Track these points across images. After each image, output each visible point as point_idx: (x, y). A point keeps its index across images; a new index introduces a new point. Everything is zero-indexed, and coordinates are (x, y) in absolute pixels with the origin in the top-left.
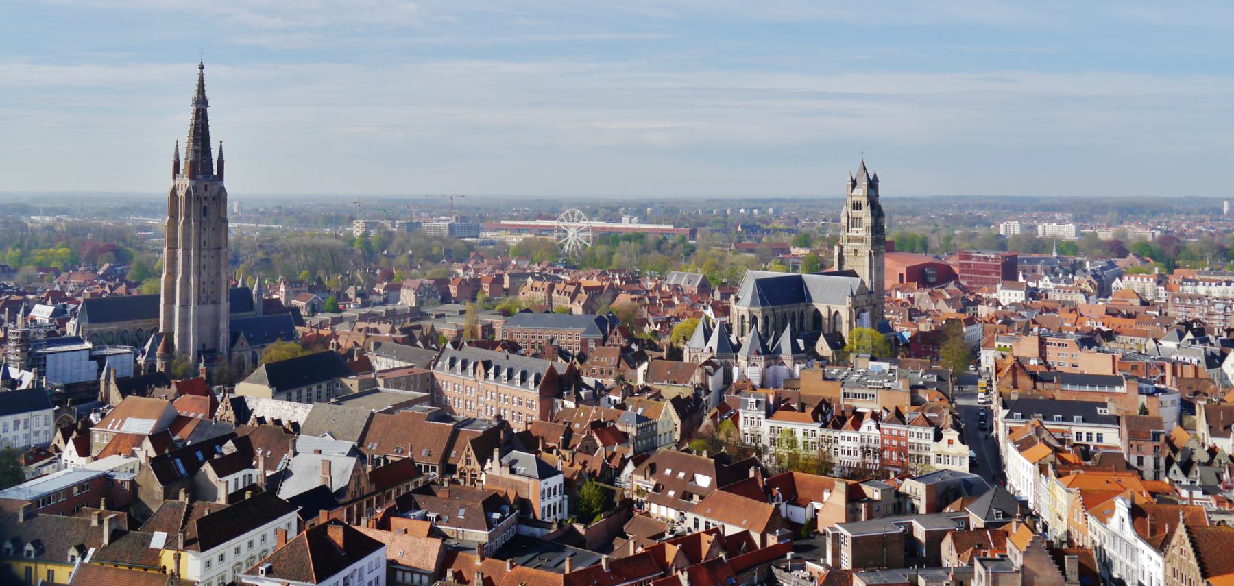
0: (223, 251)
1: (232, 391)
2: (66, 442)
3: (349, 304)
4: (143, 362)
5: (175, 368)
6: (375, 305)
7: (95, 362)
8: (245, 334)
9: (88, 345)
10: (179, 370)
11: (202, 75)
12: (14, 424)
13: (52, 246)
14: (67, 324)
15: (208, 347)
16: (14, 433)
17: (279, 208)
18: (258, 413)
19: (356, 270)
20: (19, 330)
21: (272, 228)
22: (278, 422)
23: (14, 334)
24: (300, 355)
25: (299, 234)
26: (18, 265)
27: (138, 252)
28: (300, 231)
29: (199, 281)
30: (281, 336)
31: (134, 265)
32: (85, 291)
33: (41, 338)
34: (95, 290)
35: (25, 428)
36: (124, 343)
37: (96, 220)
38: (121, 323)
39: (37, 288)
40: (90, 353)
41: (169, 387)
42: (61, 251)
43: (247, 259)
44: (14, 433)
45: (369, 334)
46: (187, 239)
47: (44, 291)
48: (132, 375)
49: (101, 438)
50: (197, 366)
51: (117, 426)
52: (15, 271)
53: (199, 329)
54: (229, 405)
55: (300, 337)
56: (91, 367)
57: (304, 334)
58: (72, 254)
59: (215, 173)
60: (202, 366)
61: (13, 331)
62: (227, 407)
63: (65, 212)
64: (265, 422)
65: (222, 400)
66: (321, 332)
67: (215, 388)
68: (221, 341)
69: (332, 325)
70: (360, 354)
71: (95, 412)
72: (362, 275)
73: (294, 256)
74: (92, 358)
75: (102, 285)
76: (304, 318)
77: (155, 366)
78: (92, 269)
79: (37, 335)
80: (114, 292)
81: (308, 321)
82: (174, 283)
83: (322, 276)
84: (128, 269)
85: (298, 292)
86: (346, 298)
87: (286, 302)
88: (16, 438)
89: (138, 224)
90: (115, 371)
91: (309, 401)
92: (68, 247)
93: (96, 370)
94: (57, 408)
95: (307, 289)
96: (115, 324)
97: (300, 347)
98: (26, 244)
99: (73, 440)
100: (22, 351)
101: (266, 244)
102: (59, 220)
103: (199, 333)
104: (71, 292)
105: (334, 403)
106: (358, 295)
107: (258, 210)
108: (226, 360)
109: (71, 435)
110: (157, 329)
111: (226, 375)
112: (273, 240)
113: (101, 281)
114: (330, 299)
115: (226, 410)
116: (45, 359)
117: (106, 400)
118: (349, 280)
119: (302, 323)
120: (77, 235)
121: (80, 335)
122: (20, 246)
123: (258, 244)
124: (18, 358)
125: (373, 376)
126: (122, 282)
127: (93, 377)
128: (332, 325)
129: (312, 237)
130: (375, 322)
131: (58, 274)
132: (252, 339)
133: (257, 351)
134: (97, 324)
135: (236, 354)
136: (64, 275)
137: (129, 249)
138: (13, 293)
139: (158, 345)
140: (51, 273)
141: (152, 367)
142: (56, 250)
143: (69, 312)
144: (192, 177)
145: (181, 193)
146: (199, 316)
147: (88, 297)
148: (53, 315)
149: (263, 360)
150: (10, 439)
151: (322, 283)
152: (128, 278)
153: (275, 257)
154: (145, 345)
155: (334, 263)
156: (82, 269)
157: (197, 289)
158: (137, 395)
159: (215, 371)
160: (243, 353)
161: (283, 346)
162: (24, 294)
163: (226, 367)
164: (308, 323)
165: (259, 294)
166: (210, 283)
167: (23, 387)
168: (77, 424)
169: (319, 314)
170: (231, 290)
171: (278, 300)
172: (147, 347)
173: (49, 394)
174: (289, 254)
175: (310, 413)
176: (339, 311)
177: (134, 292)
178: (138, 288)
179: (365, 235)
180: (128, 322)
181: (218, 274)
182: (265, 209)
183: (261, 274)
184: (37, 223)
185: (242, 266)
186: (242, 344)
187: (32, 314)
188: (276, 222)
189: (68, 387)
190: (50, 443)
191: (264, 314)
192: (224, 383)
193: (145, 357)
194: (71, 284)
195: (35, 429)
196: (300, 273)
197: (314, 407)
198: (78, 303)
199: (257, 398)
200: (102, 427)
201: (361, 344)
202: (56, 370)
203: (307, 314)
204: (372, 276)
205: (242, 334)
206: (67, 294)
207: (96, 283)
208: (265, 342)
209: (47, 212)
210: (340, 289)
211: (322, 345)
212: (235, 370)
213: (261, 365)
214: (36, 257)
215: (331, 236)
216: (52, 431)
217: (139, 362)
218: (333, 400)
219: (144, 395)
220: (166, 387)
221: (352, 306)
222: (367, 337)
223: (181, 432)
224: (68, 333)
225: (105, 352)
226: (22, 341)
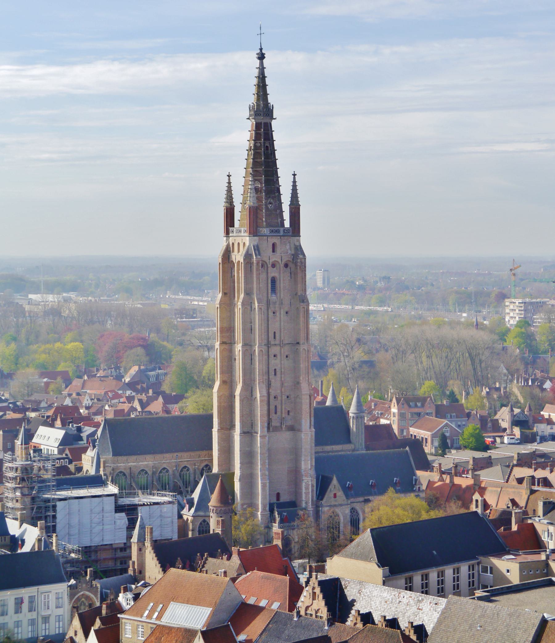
0: (303, 347)
1: (322, 569)
2: (86, 635)
3: (501, 437)
4: (190, 518)
5: (237, 528)
6: (543, 439)
7: (123, 514)
8: (339, 481)
9: (113, 489)
10: (242, 533)
11: (262, 69)
12: (16, 604)
13: (59, 340)
14: (83, 456)
15: (284, 498)
16: (16, 617)
17: (387, 279)
18: (361, 606)
19: (511, 381)
20: (20, 462)
21: (375, 313)
22: (393, 623)
23: (11, 469)
24: (425, 516)
25: (418, 322)
26: (13, 367)
27: (180, 348)
28: (420, 317)
29: (269, 394)
30: (394, 485)
31: (173, 369)
32: (107, 407)
33: (48, 476)
34: (120, 407)
35: (30, 610)
36: (163, 487)
37: (117, 300)
38: (158, 456)
39: (40, 402)
40: (116, 502)
41: (229, 558)
42: (70, 346)
43: (339, 361)
44: (16, 617)
45: (536, 488)
46: (248, 330)
47: (50, 407)
48: (175, 537)
49: (135, 632)
50: (269, 528)
51: (156, 614)
52: (10, 376)
53: (270, 470)
54: (318, 590)
55: (424, 487)
56: (118, 522)
57: (430, 483)
58: (86, 351)
59: (287, 224)
60: (276, 528)
61: (10, 465)
62: (314, 593)
63: (74, 288)
64: (373, 622)
65: (307, 583)
66: (458, 481)
67: (296, 563)
68: (304, 490)
69: (474, 470)
70: (521, 522)
71: (126, 590)
72: (521, 389)
73: (411, 357)
74: (119, 509)
75: (130, 399)
76: (430, 458)
77: (208, 524)
78: (114, 374)
79: (42, 472)
80: (147, 409)
81: (436, 462)
82: (232, 397)
83: (456, 390)
84: (166, 374)
85: (419, 414)
86: (497, 428)
87: (401, 431)
88: (18, 624)
89: (176, 306)
90: (151, 529)
91: (441, 592)
92: (82, 341)
93: (125, 527)
94: (73, 582)
95: (432, 410)
96: (148, 457)
97: (424, 504)
98: (23, 336)
99: (96, 631)
100: (23, 495)
101: (367, 337)
102: (66, 300)
103: (271, 477)
104: (87, 408)
105: (480, 598)
106: (517, 422)
107: (353, 283)
108: (311, 519)
109: (93, 624)
110: (209, 467)
111: (311, 544)
112: (377, 331)
113: (128, 393)
114: (470, 428)
115: (314, 599)
116: (54, 507)
117: (141, 572)
118: (500, 397)
119: (427, 466)
120: (91, 322)
121: (102, 473)
122: (15, 339)
123: (355, 336)
124: (18, 505)
125: (543, 557)
126: (157, 393)
127: (120, 539)
128: (474, 470)
129: (439, 326)
130: (544, 468)
131: (68, 382)
132: (350, 488)
133: (358, 507)
134: (125, 458)
135: (325, 511)
136: (77, 383)
137: (165, 343)
138: (8, 408)
139: (212, 493)
140: (59, 379)
141: (204, 526)
142: (65, 345)
143: (85, 438)
144: (254, 231)
145: (238, 257)
146: (269, 450)
147: (110, 416)
148: (65, 442)
149: (367, 522)
150: (11, 625)
151: (457, 401)
152: (166, 388)
153: (381, 357)
154: (192, 492)
155: (474, 369)
156: (100, 373)
157: (266, 408)
158: (183, 568)
159: (295, 536)
160: (338, 510)
161: (397, 502)
162: (23, 410)
163: (312, 531)
164: (436, 465)
165: (359, 417)
166: (284, 397)
167: (26, 548)
168: (100, 608)
169: (454, 451)
170: (315, 409)
171: (388, 427)
172: (196, 495)
173: (61, 560)
174: (404, 352)
175: (443, 613)
176: (486, 448)
177: (176, 410)
178: (180, 404)
179: (525, 323)
180: (167, 455)
181: (297, 384)
182: (365, 281)
183: (362, 384)
184: (38, 304)
185: (332, 372)
186: (335, 496)
187: (35, 440)
188: (382, 302)
189: (87, 551)
190: (64, 635)
191: (367, 448)
192: (309, 556)
193: (193, 510)
194: (87, 397)
195: (45, 613)
196: (421, 385)
197: (448, 603)
198: (97, 425)
199: (361, 583)
200: (136, 615)
201: (522, 503)
202: (70, 526)
203: (433, 451)
204: (537, 391)
205: (335, 481)
206: (81, 411)
207: (120, 396)
208: (371, 494)
209: (50, 288)
210: (485, 413)
211: (460, 503)
212: (325, 536)
213: (365, 530)
214: (37, 356)
215: (468, 325)
216: (67, 616)
217: (185, 517)
218: (479, 593)
219: (193, 568)
220: (225, 557)
221: (506, 440)
222: (532, 492)
223: (248, 629)
224: (85, 469)
225: (136, 500)
226: (23, 480)
